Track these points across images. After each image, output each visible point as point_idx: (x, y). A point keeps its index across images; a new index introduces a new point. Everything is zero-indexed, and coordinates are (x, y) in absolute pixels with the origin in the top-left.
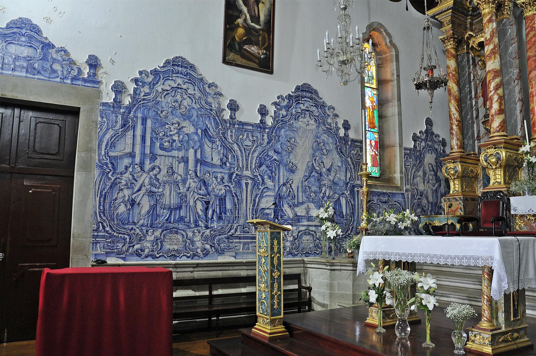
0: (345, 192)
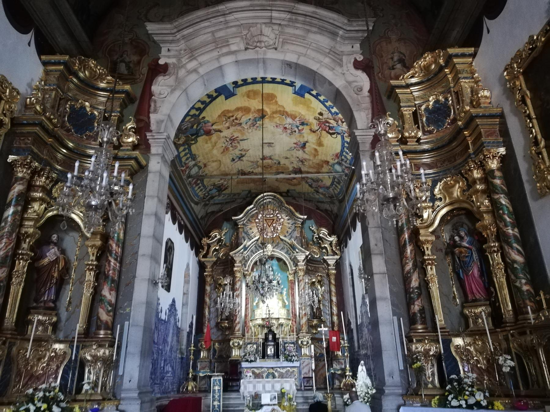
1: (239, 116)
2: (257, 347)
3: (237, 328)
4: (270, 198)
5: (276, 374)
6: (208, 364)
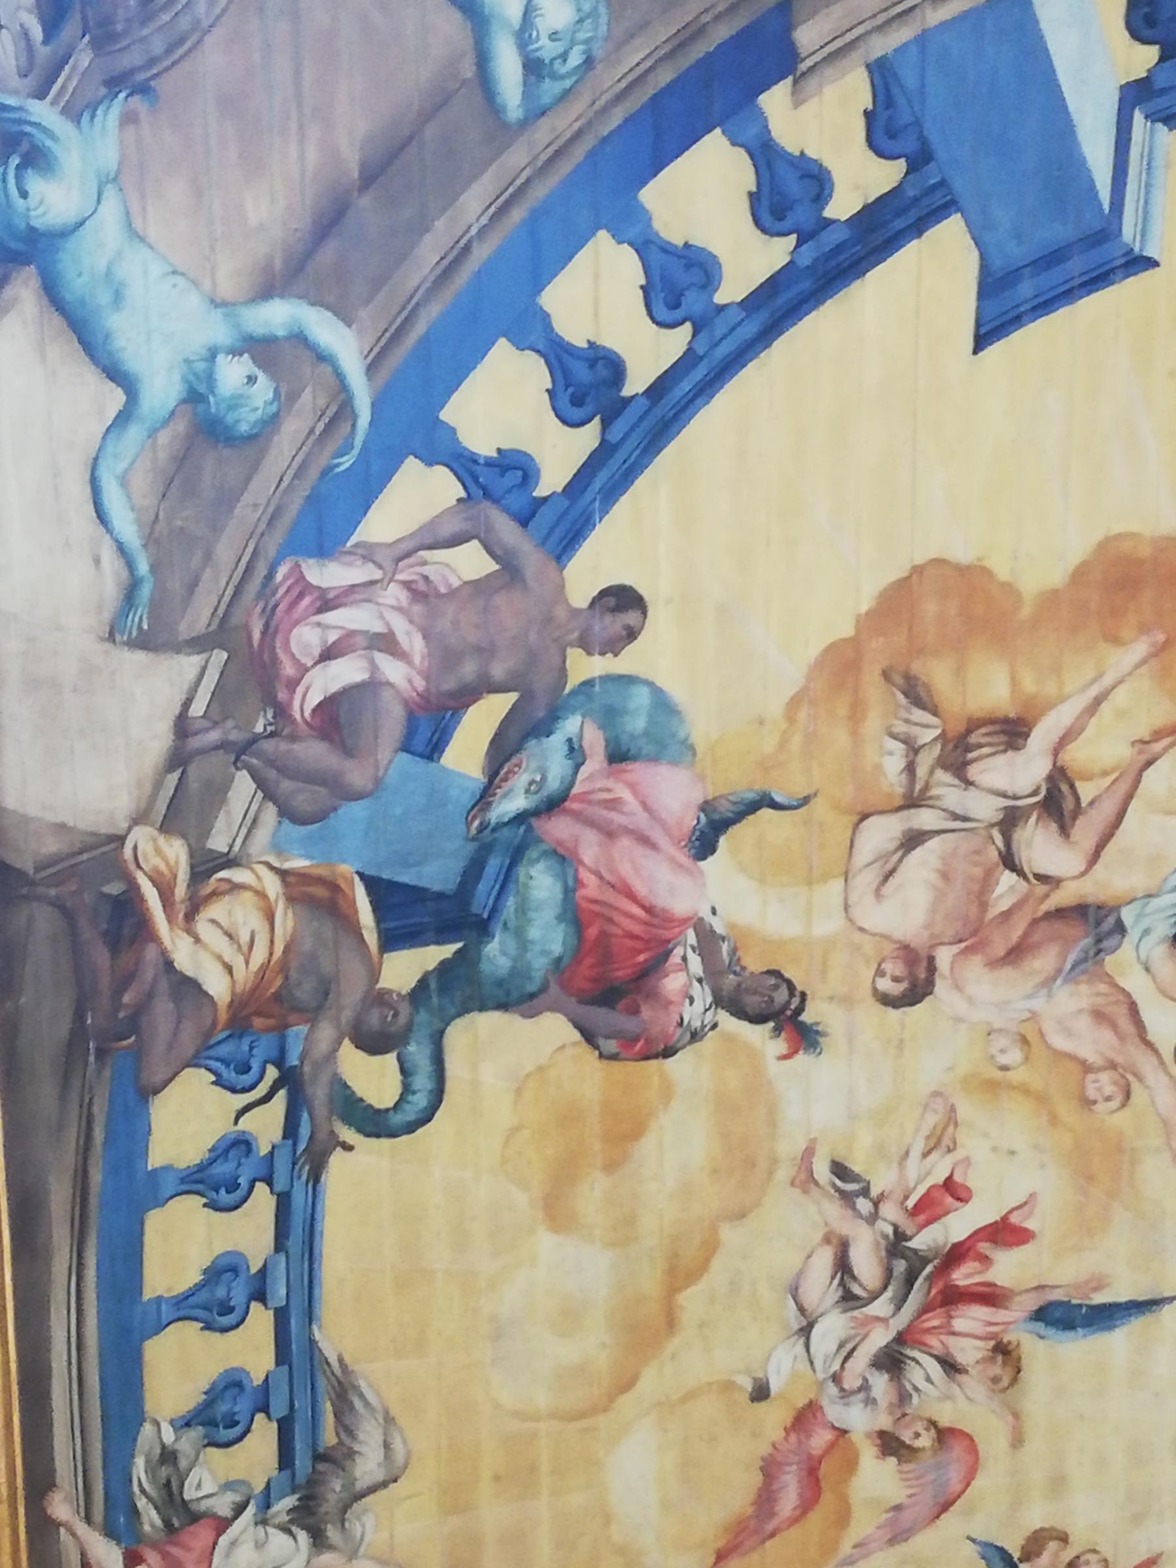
1: (1102, 750)
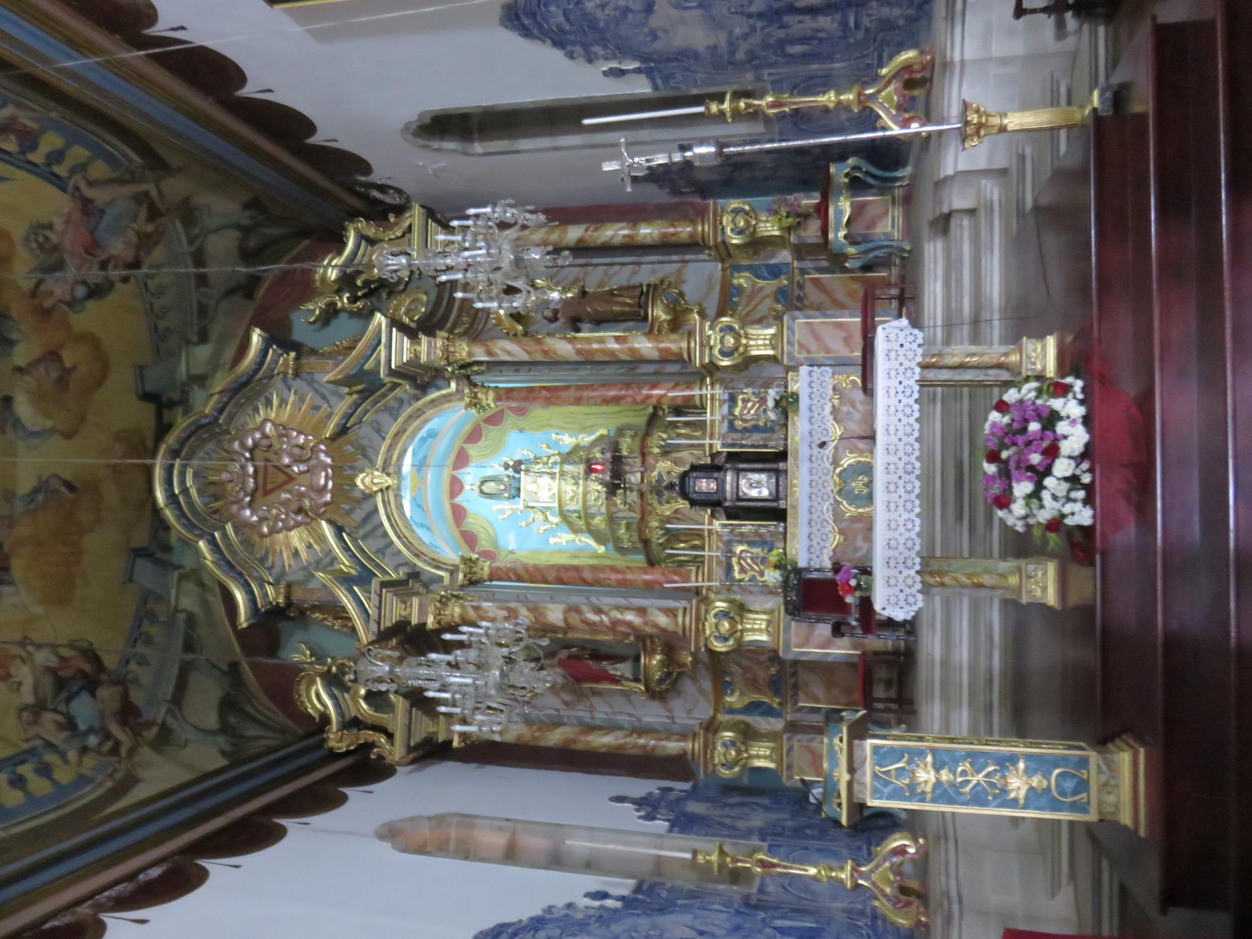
0: (759, 918)
2: (742, 539)
3: (663, 620)
4: (182, 475)
5: (848, 461)
6: (800, 740)
